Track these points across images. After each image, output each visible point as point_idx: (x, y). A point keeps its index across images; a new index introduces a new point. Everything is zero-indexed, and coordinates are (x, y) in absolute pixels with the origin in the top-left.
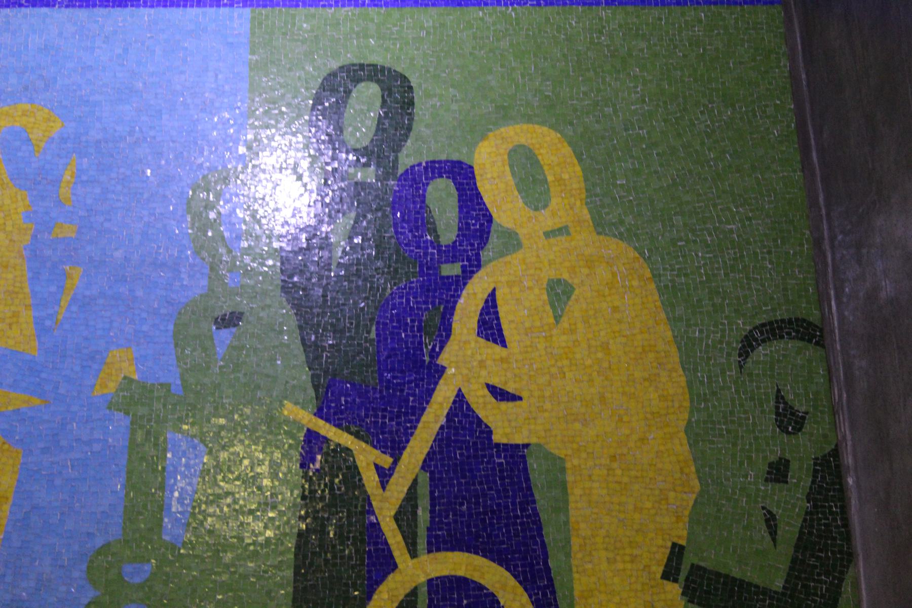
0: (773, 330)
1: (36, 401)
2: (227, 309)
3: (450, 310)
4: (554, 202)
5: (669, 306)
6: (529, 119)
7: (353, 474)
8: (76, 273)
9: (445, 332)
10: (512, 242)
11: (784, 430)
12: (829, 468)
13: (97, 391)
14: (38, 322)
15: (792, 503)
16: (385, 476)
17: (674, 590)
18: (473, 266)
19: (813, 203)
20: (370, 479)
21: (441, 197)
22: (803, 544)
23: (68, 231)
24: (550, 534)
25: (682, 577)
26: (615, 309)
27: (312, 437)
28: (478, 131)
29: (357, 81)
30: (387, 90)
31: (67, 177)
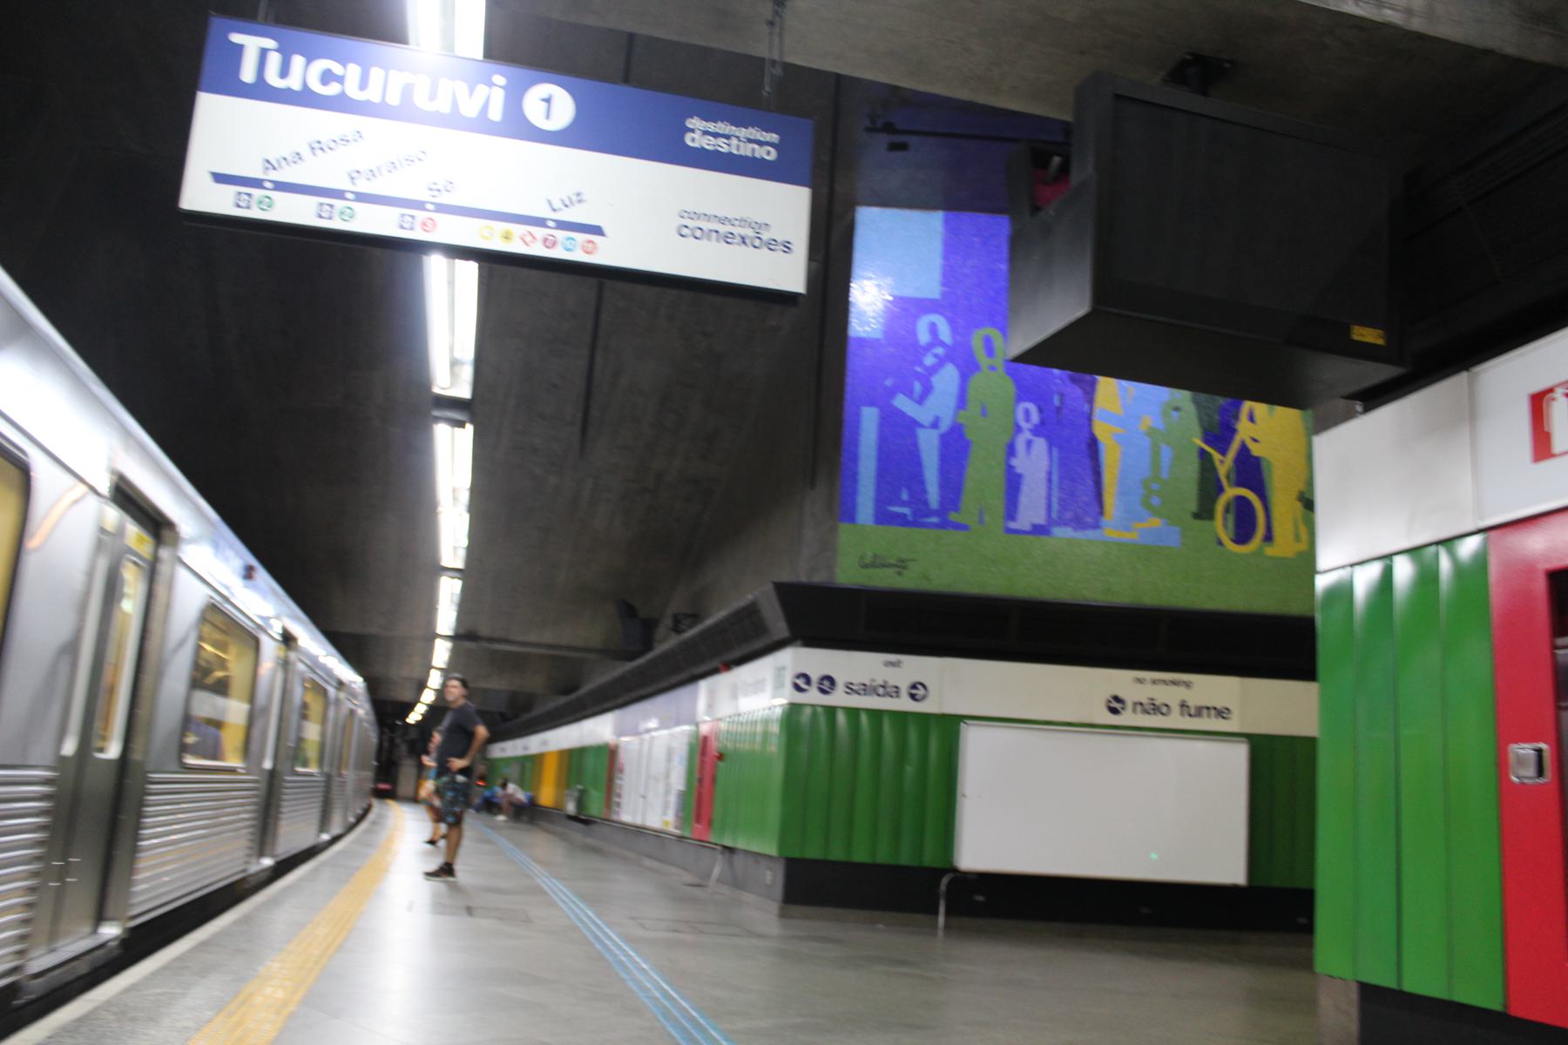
9: (1237, 418)
20: (1217, 463)
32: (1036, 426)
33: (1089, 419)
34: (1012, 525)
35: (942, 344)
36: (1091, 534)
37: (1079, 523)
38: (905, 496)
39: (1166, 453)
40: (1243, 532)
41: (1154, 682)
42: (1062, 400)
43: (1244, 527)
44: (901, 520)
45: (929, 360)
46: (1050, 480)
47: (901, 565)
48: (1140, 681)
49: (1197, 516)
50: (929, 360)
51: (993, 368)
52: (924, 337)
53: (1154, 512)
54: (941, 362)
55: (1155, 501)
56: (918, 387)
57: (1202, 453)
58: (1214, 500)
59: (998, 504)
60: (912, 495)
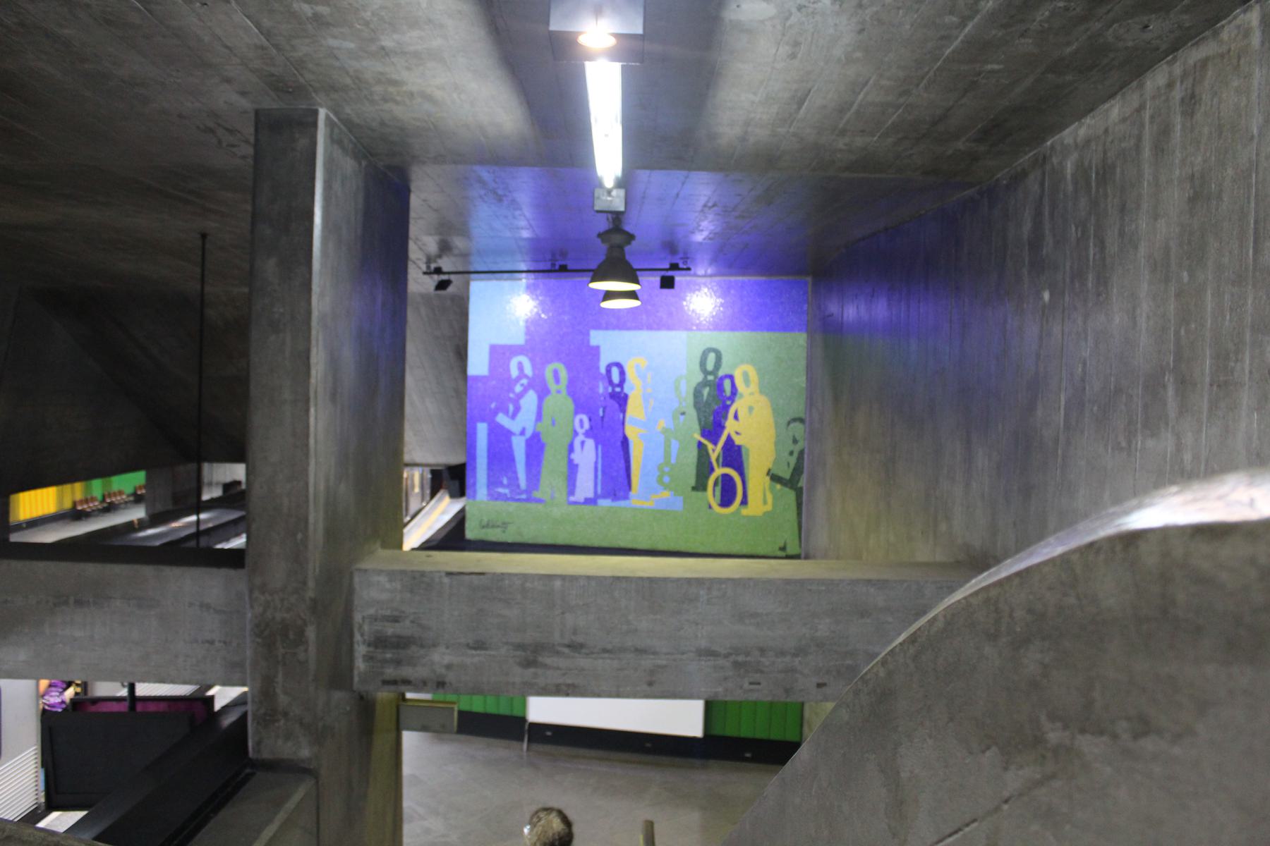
0: (794, 420)
8: (652, 402)
9: (726, 418)
15: (793, 460)
17: (768, 478)
18: (733, 401)
22: (795, 469)
23: (649, 390)
24: (745, 465)
33: (623, 423)
34: (572, 499)
35: (526, 376)
36: (622, 503)
39: (675, 445)
40: (726, 500)
43: (727, 494)
45: (518, 389)
47: (505, 525)
49: (694, 489)
50: (518, 389)
51: (559, 392)
52: (514, 372)
53: (666, 487)
54: (525, 390)
55: (666, 479)
56: (511, 408)
57: (700, 444)
58: (707, 478)
60: (509, 479)
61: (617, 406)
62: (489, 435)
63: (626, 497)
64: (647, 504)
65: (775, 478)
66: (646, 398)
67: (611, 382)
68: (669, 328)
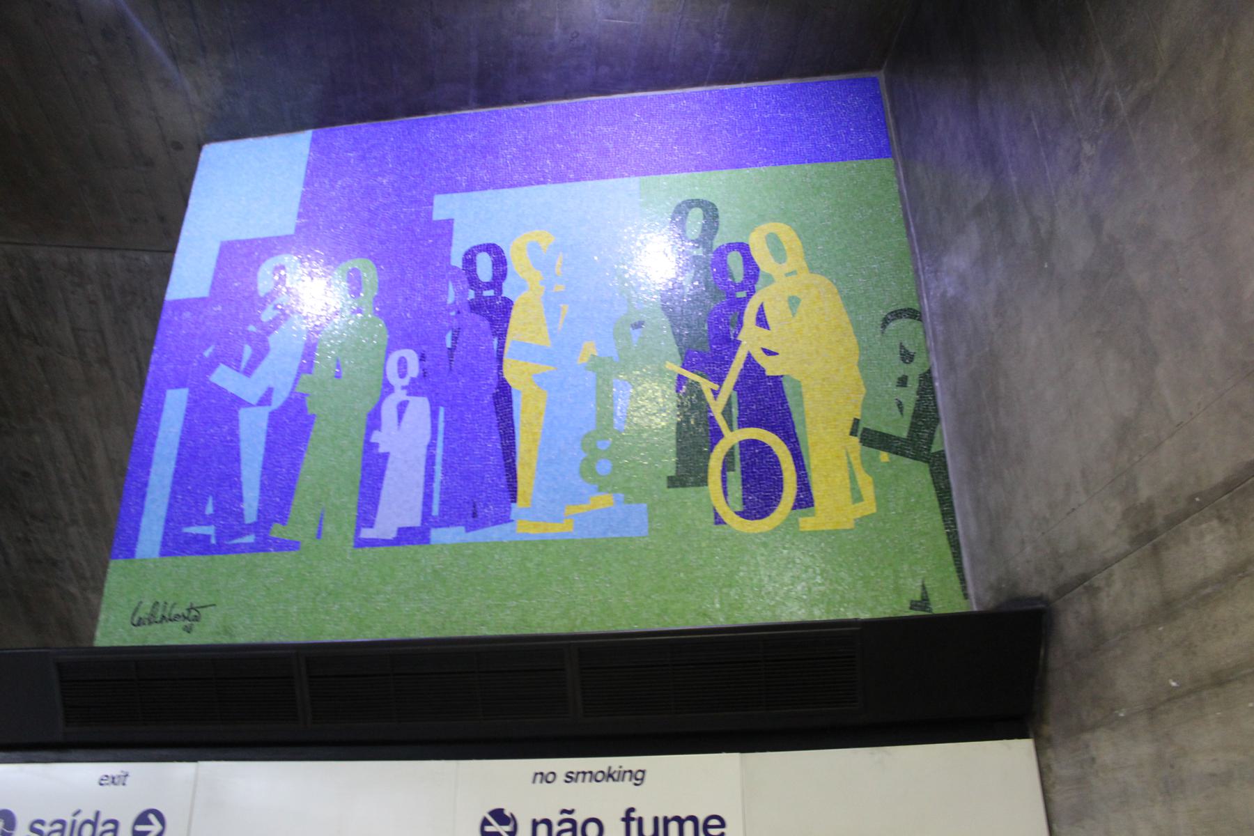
0: (897, 314)
1: (552, 368)
2: (637, 320)
3: (742, 314)
4: (789, 259)
5: (847, 306)
6: (774, 220)
7: (700, 394)
8: (565, 308)
9: (740, 323)
10: (770, 279)
11: (904, 360)
12: (927, 379)
13: (580, 362)
14: (550, 332)
15: (909, 396)
16: (715, 393)
17: (856, 440)
19: (913, 252)
21: (735, 262)
22: (916, 415)
23: (560, 288)
24: (796, 417)
25: (859, 433)
26: (821, 309)
27: (680, 377)
28: (750, 228)
29: (691, 207)
30: (706, 211)
31: (559, 263)
32: (413, 380)
33: (500, 359)
34: (367, 533)
36: (494, 533)
37: (474, 520)
38: (209, 510)
41: (570, 777)
42: (455, 339)
43: (760, 485)
44: (201, 546)
46: (430, 460)
47: (193, 615)
48: (544, 777)
49: (673, 482)
55: (604, 467)
56: (248, 352)
59: (350, 503)
61: (485, 324)
62: (189, 410)
63: (504, 519)
64: (555, 529)
65: (872, 439)
66: (551, 304)
67: (473, 281)
68: (600, 176)
